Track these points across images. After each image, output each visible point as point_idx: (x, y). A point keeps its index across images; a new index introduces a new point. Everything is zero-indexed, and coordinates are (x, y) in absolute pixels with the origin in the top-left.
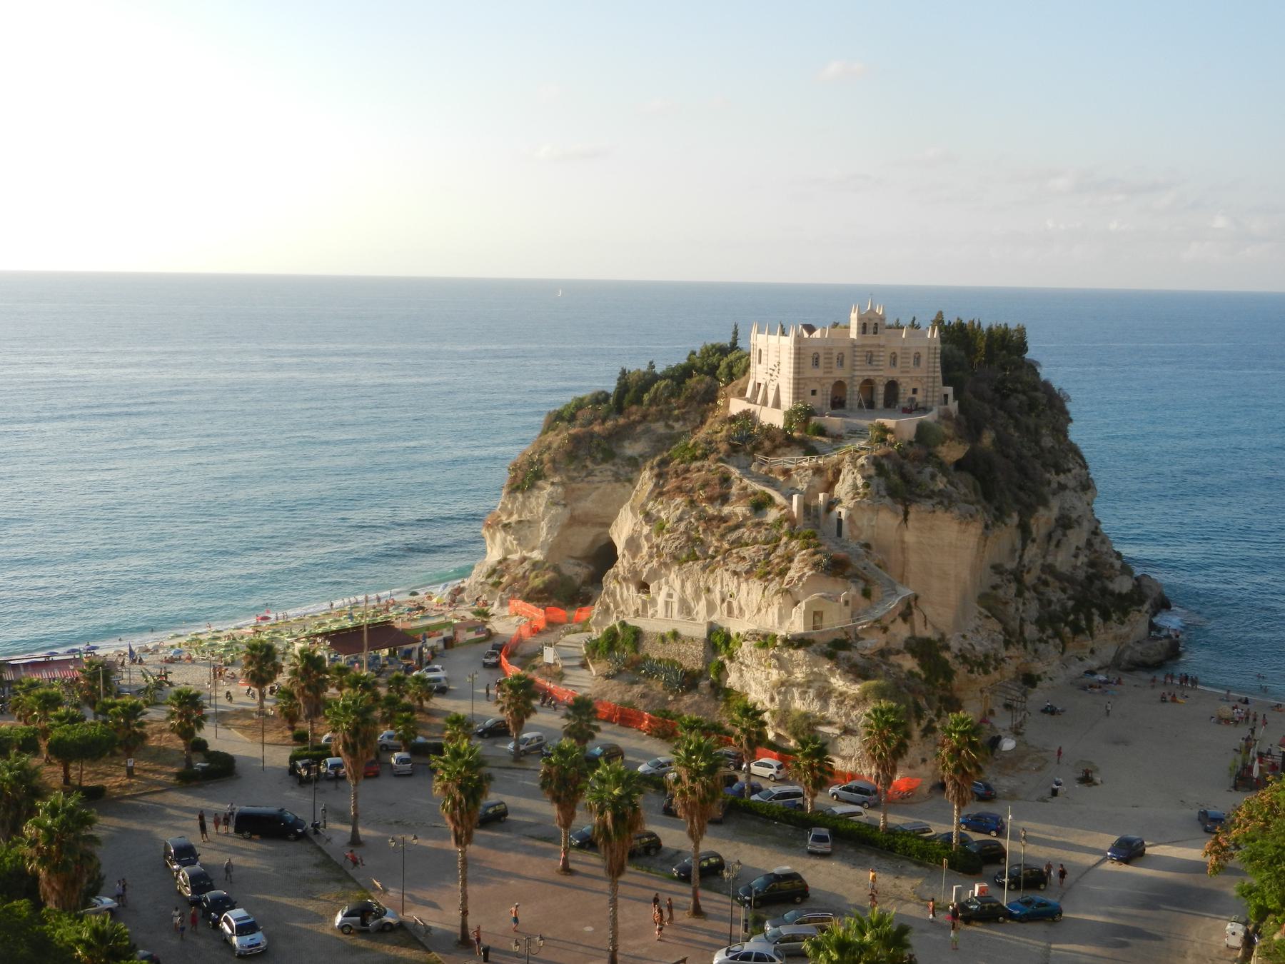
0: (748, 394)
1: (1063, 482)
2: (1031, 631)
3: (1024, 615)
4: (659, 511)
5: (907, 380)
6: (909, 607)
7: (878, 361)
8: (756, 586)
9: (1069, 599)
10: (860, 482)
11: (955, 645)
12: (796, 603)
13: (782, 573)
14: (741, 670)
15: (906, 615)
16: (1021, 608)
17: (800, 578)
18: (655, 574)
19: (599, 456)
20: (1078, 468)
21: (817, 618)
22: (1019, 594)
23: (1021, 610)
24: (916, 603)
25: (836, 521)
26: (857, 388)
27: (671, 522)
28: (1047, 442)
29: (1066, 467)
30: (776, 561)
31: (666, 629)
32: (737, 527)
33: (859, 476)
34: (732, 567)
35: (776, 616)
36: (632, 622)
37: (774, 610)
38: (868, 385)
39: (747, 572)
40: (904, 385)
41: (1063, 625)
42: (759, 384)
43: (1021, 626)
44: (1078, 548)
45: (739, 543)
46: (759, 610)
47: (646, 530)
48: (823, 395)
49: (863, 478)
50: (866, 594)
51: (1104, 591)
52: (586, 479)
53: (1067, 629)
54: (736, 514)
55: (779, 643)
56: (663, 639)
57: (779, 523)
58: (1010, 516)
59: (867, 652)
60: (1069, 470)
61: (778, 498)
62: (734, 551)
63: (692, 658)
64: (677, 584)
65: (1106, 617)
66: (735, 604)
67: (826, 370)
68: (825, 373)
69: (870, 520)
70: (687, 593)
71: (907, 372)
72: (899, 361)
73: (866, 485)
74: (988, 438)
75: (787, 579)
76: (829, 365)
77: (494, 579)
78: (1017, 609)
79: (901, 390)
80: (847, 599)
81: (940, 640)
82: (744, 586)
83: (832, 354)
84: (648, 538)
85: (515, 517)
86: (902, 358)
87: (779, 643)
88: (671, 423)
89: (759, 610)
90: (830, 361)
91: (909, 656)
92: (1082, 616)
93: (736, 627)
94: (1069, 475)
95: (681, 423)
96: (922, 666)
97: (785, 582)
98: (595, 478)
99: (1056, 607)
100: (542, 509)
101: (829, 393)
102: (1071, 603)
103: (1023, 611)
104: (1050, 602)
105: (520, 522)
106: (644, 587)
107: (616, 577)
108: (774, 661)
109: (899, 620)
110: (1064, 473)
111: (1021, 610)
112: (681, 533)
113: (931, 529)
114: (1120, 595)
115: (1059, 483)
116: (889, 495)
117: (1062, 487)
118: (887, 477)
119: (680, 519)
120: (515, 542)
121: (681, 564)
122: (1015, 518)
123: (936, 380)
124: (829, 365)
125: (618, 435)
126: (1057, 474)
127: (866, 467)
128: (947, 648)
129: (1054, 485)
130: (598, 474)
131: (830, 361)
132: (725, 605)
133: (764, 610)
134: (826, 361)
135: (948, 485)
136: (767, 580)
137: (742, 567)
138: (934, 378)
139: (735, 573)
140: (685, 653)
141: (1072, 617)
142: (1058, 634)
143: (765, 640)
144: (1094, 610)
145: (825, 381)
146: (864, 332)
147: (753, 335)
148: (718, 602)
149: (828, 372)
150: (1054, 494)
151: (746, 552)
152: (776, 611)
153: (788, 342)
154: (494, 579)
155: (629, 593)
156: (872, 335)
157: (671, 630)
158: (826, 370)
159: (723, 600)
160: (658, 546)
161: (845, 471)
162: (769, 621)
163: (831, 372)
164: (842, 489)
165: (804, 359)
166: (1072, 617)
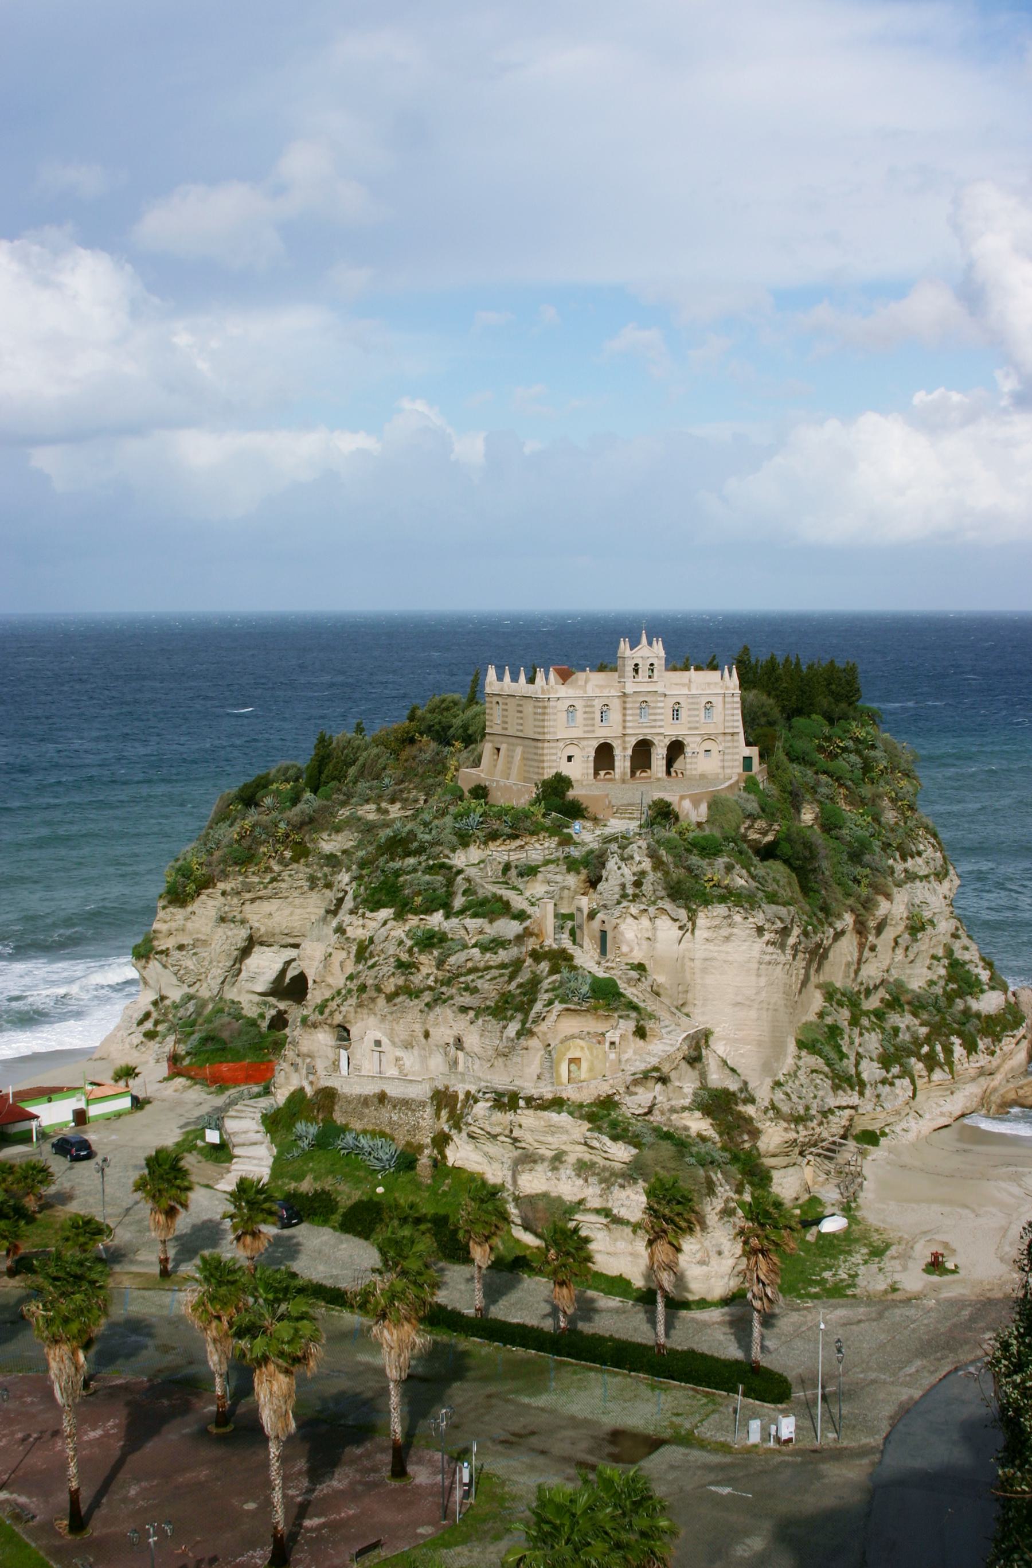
1: (911, 869)
2: (871, 1070)
3: (860, 1050)
5: (698, 739)
6: (698, 1048)
7: (655, 714)
8: (493, 1024)
9: (921, 1025)
10: (630, 879)
11: (763, 1093)
13: (524, 1009)
15: (694, 1060)
16: (857, 1041)
19: (288, 854)
20: (930, 849)
21: (573, 1067)
22: (854, 1022)
23: (857, 1044)
24: (707, 1042)
25: (598, 934)
26: (630, 752)
28: (890, 816)
29: (914, 850)
31: (371, 1089)
40: (691, 745)
41: (913, 1060)
42: (498, 750)
43: (857, 1065)
44: (934, 957)
48: (583, 762)
49: (634, 874)
50: (641, 1033)
52: (270, 886)
53: (920, 1066)
55: (522, 1103)
56: (365, 1101)
58: (839, 916)
59: (641, 1111)
60: (919, 854)
65: (971, 1048)
67: (586, 729)
68: (585, 732)
71: (696, 728)
72: (683, 714)
73: (638, 884)
74: (808, 816)
75: (533, 1014)
76: (590, 722)
77: (149, 1025)
78: (852, 1043)
79: (688, 750)
80: (613, 1040)
81: (741, 1090)
83: (593, 706)
86: (689, 710)
87: (522, 1103)
88: (384, 805)
90: (592, 716)
91: (698, 1114)
92: (938, 1048)
94: (919, 861)
95: (398, 805)
98: (283, 885)
99: (904, 1037)
101: (592, 759)
102: (924, 1031)
103: (860, 1045)
104: (896, 1030)
107: (304, 1021)
109: (684, 1065)
110: (912, 857)
111: (857, 1044)
113: (727, 939)
114: (989, 1017)
115: (906, 871)
116: (669, 896)
117: (911, 877)
118: (666, 873)
121: (390, 998)
122: (849, 919)
123: (736, 738)
124: (590, 722)
125: (311, 823)
126: (904, 859)
127: (637, 858)
128: (751, 1100)
130: (286, 878)
131: (592, 716)
134: (585, 716)
135: (750, 880)
136: (505, 1018)
138: (733, 734)
139: (464, 1009)
141: (925, 1049)
142: (907, 1073)
144: (955, 1040)
145: (585, 743)
149: (588, 732)
150: (899, 885)
154: (149, 1025)
155: (323, 1039)
156: (647, 679)
157: (377, 1090)
158: (586, 729)
163: (593, 731)
165: (555, 714)
166: (925, 1049)
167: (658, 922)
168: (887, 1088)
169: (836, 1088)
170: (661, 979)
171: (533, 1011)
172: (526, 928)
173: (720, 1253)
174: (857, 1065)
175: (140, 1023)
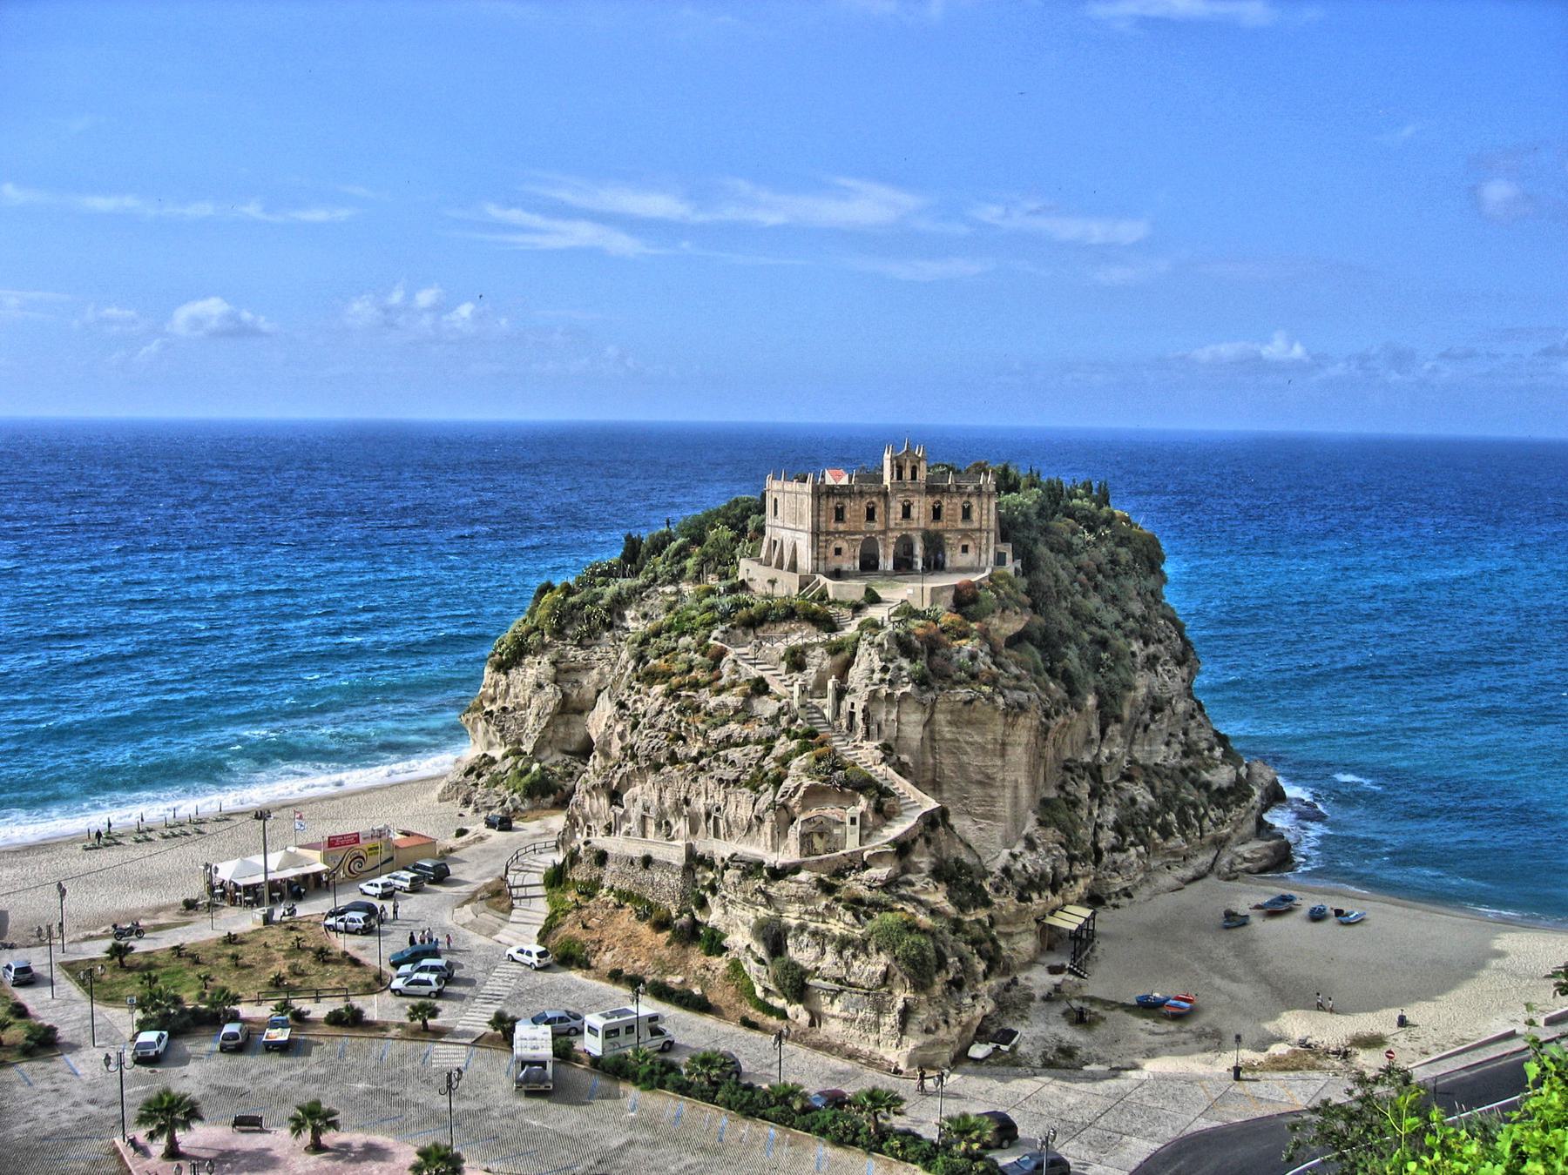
0: (763, 555)
2: (1107, 838)
3: (1099, 821)
4: (635, 702)
10: (878, 664)
12: (793, 820)
13: (778, 781)
14: (725, 907)
16: (1095, 813)
17: (797, 789)
18: (627, 781)
27: (648, 715)
30: (773, 765)
32: (725, 723)
33: (876, 658)
34: (717, 773)
35: (769, 837)
36: (600, 841)
37: (767, 827)
38: (906, 544)
39: (736, 781)
42: (775, 542)
44: (1171, 735)
45: (728, 742)
46: (750, 828)
47: (619, 728)
49: (881, 660)
50: (878, 810)
51: (1207, 786)
53: (1155, 835)
54: (726, 706)
55: (765, 873)
57: (774, 720)
61: (775, 687)
62: (721, 753)
63: (666, 889)
64: (655, 795)
66: (722, 823)
69: (888, 713)
70: (666, 805)
73: (885, 670)
75: (782, 789)
78: (1090, 813)
82: (732, 798)
84: (622, 736)
85: (500, 703)
89: (750, 828)
93: (721, 849)
96: (950, 897)
97: (779, 794)
100: (528, 692)
105: (504, 709)
106: (615, 797)
108: (760, 898)
112: (660, 730)
114: (1220, 790)
119: (660, 712)
120: (498, 734)
127: (886, 646)
129: (1139, 660)
132: (711, 821)
133: (755, 829)
135: (994, 667)
137: (730, 774)
140: (659, 884)
143: (752, 868)
146: (900, 477)
147: (768, 482)
148: (704, 817)
151: (735, 754)
152: (769, 831)
153: (808, 487)
159: (708, 815)
160: (632, 747)
161: (860, 652)
162: (758, 848)
164: (856, 675)
167: (904, 706)
168: (1124, 856)
169: (1072, 859)
170: (905, 758)
171: (784, 784)
172: (780, 709)
173: (946, 1022)
174: (1095, 834)
175: (466, 775)
